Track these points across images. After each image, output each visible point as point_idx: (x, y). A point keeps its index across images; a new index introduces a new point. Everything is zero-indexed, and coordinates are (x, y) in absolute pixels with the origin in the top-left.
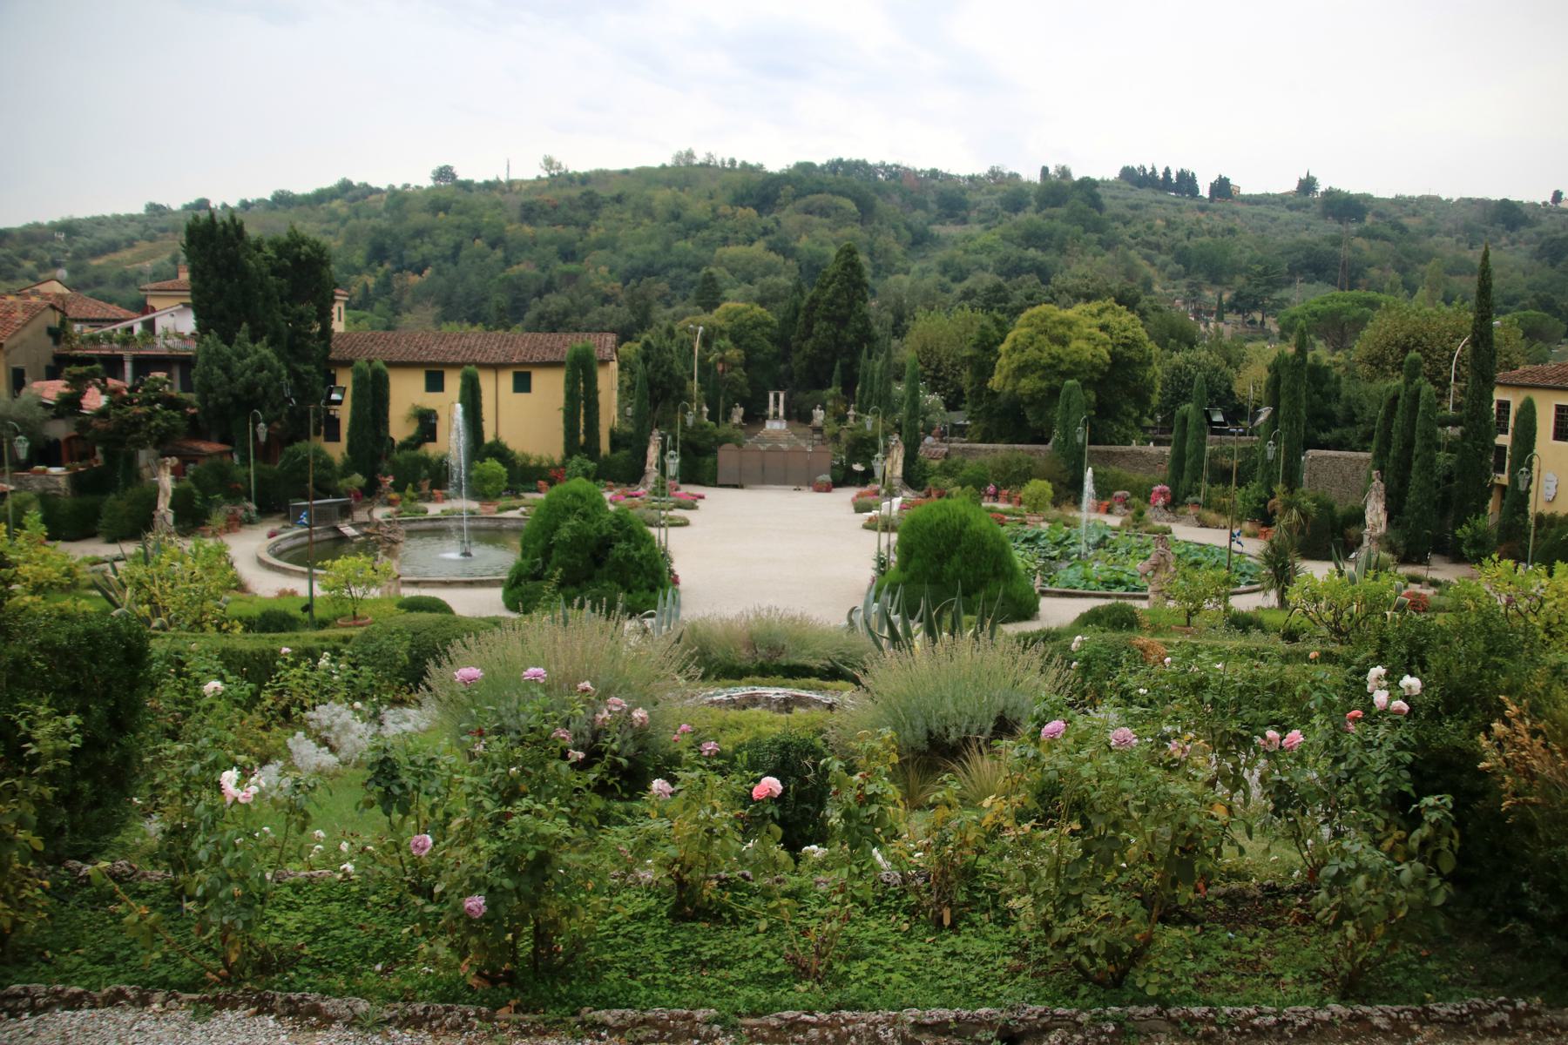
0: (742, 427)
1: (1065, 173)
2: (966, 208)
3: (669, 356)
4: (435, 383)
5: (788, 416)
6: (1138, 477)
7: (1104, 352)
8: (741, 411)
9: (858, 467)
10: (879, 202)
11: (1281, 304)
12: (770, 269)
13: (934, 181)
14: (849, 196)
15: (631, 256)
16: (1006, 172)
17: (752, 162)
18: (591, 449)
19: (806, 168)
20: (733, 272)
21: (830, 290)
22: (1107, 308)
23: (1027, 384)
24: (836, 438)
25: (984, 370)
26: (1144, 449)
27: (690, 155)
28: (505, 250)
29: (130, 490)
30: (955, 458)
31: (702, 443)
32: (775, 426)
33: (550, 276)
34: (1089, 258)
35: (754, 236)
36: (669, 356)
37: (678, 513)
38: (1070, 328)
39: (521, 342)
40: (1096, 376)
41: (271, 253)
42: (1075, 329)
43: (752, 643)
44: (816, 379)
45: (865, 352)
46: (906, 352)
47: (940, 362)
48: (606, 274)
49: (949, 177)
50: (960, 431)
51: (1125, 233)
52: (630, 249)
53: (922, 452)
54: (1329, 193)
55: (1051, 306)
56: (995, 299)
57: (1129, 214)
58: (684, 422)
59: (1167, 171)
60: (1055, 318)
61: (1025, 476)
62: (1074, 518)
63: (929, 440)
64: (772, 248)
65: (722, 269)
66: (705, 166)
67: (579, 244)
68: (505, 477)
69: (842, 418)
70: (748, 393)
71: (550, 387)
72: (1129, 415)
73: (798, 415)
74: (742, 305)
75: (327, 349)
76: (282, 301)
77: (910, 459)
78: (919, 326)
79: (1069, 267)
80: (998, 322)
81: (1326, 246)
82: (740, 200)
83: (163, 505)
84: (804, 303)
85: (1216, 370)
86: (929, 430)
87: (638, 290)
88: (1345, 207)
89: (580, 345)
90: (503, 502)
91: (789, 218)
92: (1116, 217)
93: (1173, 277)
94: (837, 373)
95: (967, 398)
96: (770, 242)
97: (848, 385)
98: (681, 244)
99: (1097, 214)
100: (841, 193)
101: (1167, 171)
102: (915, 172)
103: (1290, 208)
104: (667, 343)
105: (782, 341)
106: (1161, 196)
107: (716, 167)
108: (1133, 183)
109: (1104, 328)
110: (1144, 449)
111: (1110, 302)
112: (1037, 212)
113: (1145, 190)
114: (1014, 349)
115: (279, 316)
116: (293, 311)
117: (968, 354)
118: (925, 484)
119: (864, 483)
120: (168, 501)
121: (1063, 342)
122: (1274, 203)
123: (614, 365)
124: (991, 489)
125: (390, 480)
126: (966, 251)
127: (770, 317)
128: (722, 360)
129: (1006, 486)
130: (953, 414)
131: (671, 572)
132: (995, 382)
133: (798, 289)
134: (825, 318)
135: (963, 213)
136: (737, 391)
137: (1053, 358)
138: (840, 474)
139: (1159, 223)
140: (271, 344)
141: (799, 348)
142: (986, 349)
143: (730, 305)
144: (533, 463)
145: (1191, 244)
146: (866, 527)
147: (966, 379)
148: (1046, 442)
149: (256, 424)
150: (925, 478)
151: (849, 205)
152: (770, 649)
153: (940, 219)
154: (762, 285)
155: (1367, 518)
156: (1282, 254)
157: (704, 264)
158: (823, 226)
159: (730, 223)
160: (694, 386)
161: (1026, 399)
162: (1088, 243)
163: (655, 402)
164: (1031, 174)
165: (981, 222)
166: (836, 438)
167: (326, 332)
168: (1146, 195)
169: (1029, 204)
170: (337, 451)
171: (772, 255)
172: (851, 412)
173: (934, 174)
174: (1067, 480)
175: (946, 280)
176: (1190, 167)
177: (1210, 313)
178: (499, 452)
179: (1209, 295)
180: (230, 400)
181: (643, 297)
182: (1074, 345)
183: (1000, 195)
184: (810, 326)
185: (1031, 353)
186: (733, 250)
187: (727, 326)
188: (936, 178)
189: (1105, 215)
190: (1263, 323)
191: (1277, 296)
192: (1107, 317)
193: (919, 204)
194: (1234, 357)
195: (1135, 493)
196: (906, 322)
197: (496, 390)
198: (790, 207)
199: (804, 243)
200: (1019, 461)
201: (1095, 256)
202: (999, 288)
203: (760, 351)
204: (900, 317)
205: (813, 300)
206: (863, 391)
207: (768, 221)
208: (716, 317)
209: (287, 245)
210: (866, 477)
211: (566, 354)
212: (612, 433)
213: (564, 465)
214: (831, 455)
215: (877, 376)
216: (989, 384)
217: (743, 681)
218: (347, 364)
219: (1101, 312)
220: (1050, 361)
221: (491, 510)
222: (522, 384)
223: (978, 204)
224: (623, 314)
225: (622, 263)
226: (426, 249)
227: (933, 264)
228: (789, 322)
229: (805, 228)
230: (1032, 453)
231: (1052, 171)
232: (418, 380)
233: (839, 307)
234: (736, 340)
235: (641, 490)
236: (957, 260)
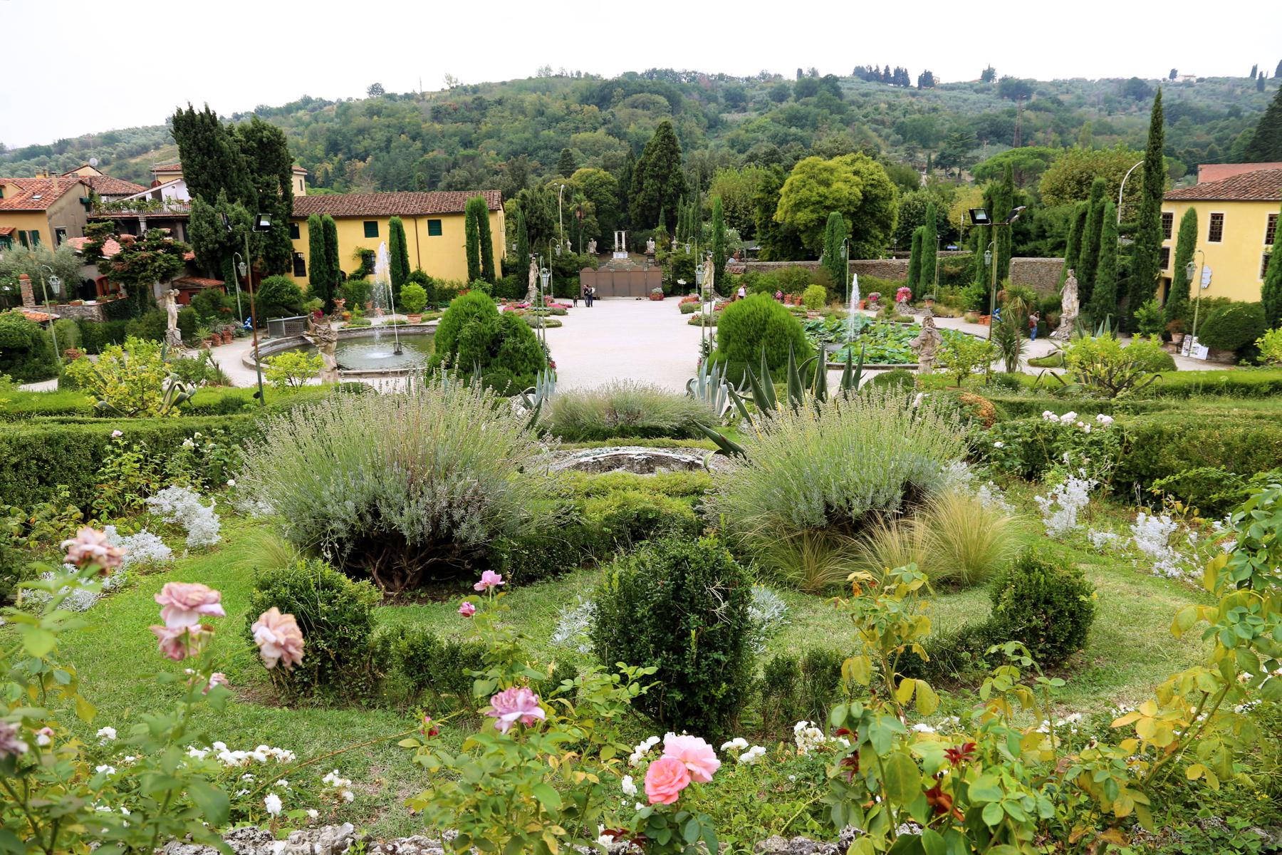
0: (596, 256)
1: (814, 73)
2: (745, 101)
4: (371, 230)
5: (628, 249)
6: (886, 282)
7: (857, 192)
8: (595, 243)
9: (681, 282)
10: (684, 98)
11: (974, 160)
12: (609, 147)
13: (722, 83)
14: (662, 94)
16: (772, 74)
17: (593, 73)
18: (488, 275)
19: (631, 75)
20: (584, 151)
21: (654, 156)
22: (858, 159)
23: (803, 216)
24: (663, 262)
25: (769, 208)
26: (889, 261)
27: (548, 69)
29: (146, 315)
30: (752, 272)
31: (569, 268)
32: (620, 256)
34: (835, 132)
35: (597, 125)
37: (553, 318)
38: (832, 174)
39: (434, 200)
40: (852, 209)
41: (240, 137)
42: (836, 174)
43: (613, 411)
44: (647, 222)
45: (681, 200)
46: (712, 199)
47: (735, 205)
49: (732, 79)
50: (754, 254)
51: (859, 113)
53: (727, 269)
54: (1004, 79)
55: (817, 158)
56: (771, 158)
57: (861, 100)
58: (554, 253)
59: (887, 69)
60: (821, 167)
61: (803, 284)
62: (841, 313)
63: (731, 260)
64: (610, 133)
65: (576, 149)
66: (559, 77)
68: (425, 296)
69: (669, 248)
70: (599, 233)
71: (455, 229)
72: (876, 238)
73: (636, 248)
74: (591, 170)
75: (289, 207)
76: (252, 172)
77: (719, 274)
78: (719, 180)
79: (820, 140)
80: (777, 173)
81: (1005, 118)
82: (585, 100)
83: (172, 324)
84: (636, 166)
85: (936, 204)
86: (731, 254)
87: (517, 164)
88: (1015, 89)
89: (474, 199)
90: (426, 315)
91: (621, 112)
92: (852, 103)
93: (894, 144)
94: (662, 216)
95: (757, 229)
96: (608, 129)
97: (671, 226)
99: (839, 101)
100: (657, 92)
101: (887, 69)
102: (708, 76)
103: (977, 91)
104: (539, 195)
105: (621, 195)
106: (883, 87)
107: (567, 77)
108: (863, 78)
109: (856, 173)
110: (889, 261)
111: (860, 154)
112: (796, 101)
113: (871, 83)
114: (791, 191)
115: (250, 184)
116: (261, 180)
117: (757, 196)
118: (731, 292)
119: (687, 294)
120: (175, 322)
121: (827, 184)
122: (965, 89)
123: (501, 214)
124: (779, 294)
125: (343, 302)
126: (747, 131)
127: (612, 178)
128: (579, 209)
129: (790, 290)
130: (747, 243)
131: (549, 359)
132: (778, 216)
133: (630, 156)
134: (652, 177)
135: (744, 104)
136: (591, 232)
137: (820, 196)
138: (669, 288)
139: (883, 106)
140: (246, 204)
141: (634, 199)
142: (770, 193)
143: (583, 170)
144: (446, 286)
145: (907, 120)
146: (690, 323)
147: (756, 216)
148: (817, 259)
149: (237, 264)
150: (730, 288)
151: (662, 100)
152: (628, 414)
153: (727, 109)
154: (604, 157)
156: (973, 124)
157: (563, 146)
159: (579, 117)
160: (559, 227)
161: (802, 228)
162: (833, 122)
163: (532, 239)
164: (790, 75)
165: (756, 110)
166: (663, 262)
167: (288, 195)
168: (873, 86)
169: (790, 95)
170: (303, 283)
172: (675, 242)
173: (721, 77)
174: (834, 286)
175: (734, 151)
176: (903, 66)
177: (922, 169)
178: (421, 279)
179: (921, 156)
180: (217, 245)
181: (521, 168)
182: (835, 186)
183: (769, 90)
184: (641, 184)
185: (804, 193)
186: (583, 136)
187: (582, 185)
188: (723, 80)
189: (844, 101)
190: (960, 175)
191: (969, 155)
192: (859, 165)
194: (947, 195)
195: (884, 294)
196: (709, 180)
197: (415, 233)
198: (621, 103)
199: (632, 129)
200: (798, 273)
201: (839, 130)
202: (774, 152)
203: (606, 203)
204: (704, 177)
205: (642, 164)
206: (681, 228)
207: (606, 114)
208: (574, 179)
209: (253, 131)
210: (687, 290)
211: (466, 206)
212: (503, 262)
213: (469, 288)
214: (660, 275)
215: (691, 217)
216: (774, 218)
217: (607, 442)
218: (304, 219)
219: (854, 161)
220: (818, 198)
221: (417, 320)
222: (435, 229)
223: (753, 97)
224: (508, 180)
227: (724, 142)
228: (625, 181)
229: (633, 118)
230: (807, 267)
231: (805, 72)
232: (359, 228)
233: (661, 168)
234: (589, 196)
235: (526, 303)
236: (741, 137)
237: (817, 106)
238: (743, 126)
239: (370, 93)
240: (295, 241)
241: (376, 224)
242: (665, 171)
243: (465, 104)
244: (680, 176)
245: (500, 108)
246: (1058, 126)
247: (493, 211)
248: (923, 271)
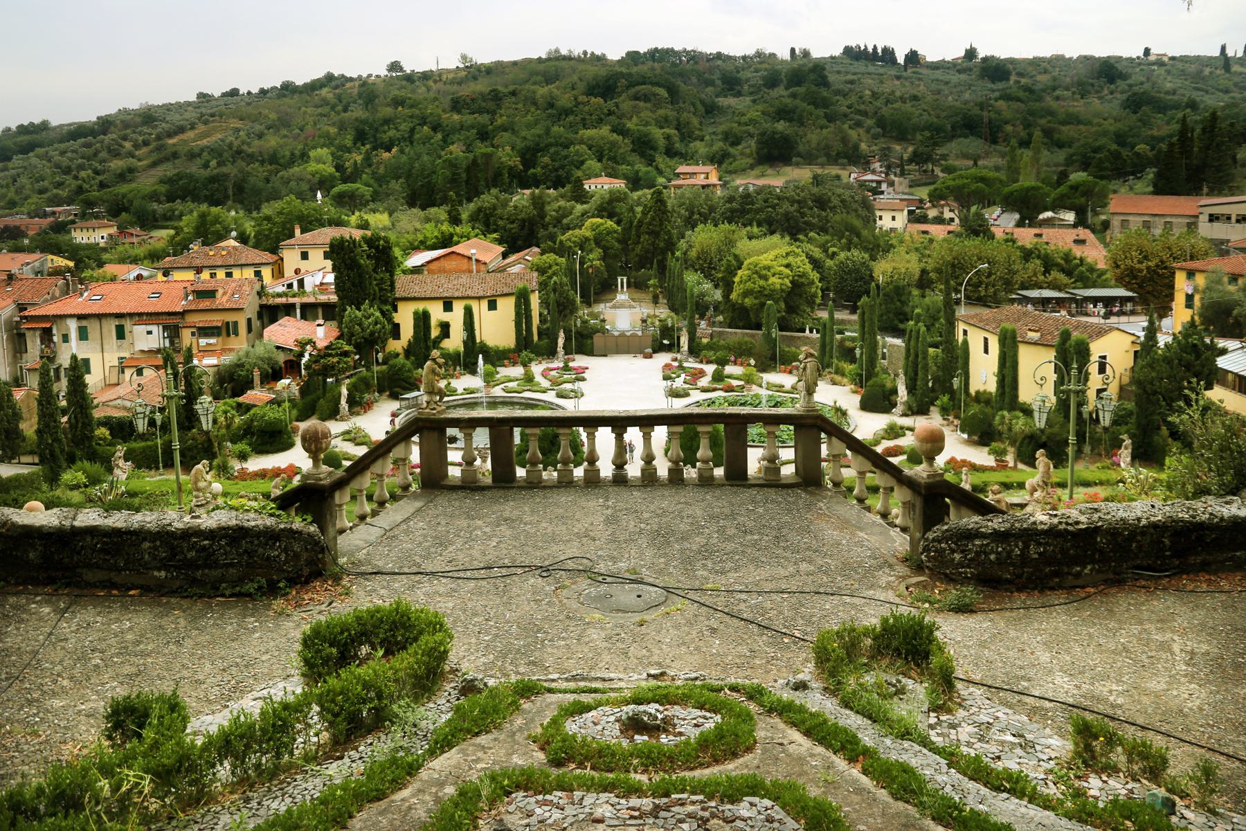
3: (566, 288)
15: (525, 138)
17: (598, 53)
28: (443, 131)
33: (475, 156)
36: (566, 288)
48: (510, 151)
51: (842, 106)
52: (523, 134)
64: (613, 131)
65: (584, 146)
67: (490, 127)
74: (599, 220)
98: (555, 129)
100: (658, 84)
132: (733, 296)
134: (647, 233)
145: (886, 111)
151: (663, 92)
153: (723, 93)
155: (899, 392)
158: (647, 109)
162: (818, 117)
165: (751, 93)
171: (615, 135)
193: (708, 83)
205: (640, 221)
207: (610, 104)
225: (520, 144)
226: (392, 133)
237: (803, 100)
238: (736, 119)
239: (389, 70)
240: (394, 314)
241: (451, 303)
242: (657, 229)
243: (482, 94)
244: (669, 233)
245: (514, 99)
246: (1025, 119)
247: (533, 291)
248: (828, 349)
